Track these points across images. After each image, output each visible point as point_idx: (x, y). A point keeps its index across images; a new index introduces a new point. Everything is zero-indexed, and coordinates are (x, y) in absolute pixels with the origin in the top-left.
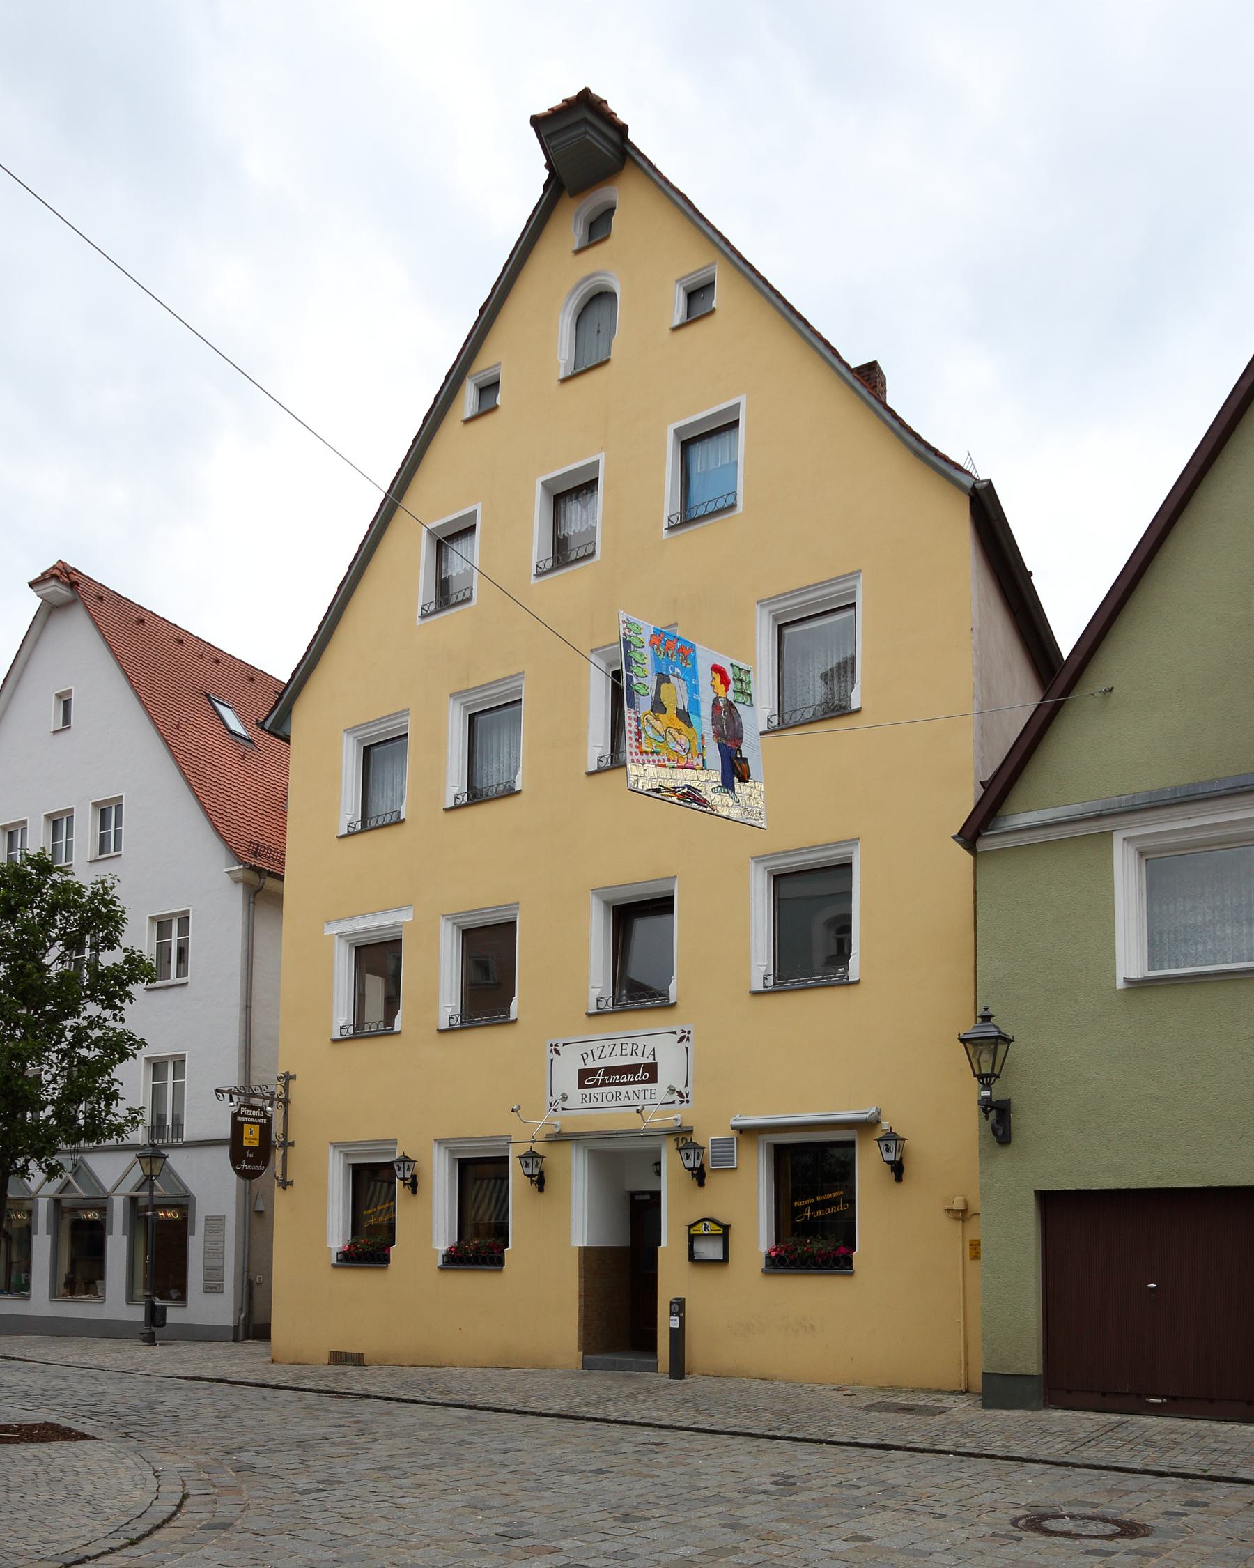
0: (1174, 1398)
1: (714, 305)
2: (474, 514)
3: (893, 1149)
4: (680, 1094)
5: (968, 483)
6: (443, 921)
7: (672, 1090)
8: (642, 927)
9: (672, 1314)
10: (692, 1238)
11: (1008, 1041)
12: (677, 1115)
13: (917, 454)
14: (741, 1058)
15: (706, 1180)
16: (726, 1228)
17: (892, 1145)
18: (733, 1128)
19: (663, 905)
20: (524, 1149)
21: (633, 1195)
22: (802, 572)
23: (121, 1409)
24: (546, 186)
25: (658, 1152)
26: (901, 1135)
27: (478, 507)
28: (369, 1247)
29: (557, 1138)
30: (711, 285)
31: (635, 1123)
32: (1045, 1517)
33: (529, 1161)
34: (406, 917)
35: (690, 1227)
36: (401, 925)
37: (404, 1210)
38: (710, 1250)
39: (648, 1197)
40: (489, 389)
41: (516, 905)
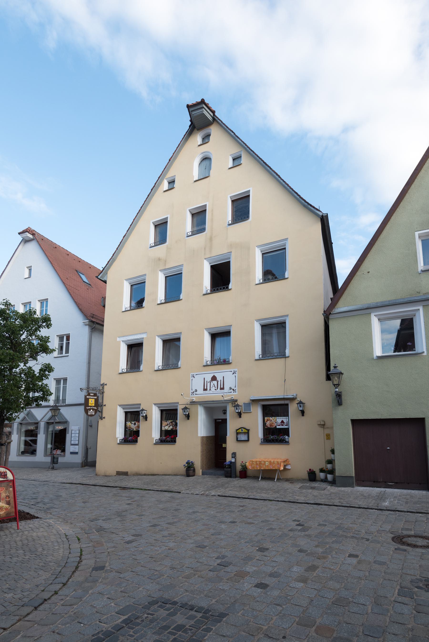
0: (397, 483)
1: (241, 162)
2: (167, 218)
3: (302, 406)
4: (233, 390)
5: (321, 214)
6: (157, 337)
7: (231, 388)
8: (218, 340)
9: (232, 458)
10: (237, 434)
11: (342, 374)
12: (233, 396)
13: (304, 206)
14: (249, 378)
15: (242, 416)
16: (248, 430)
17: (302, 405)
18: (251, 400)
19: (227, 334)
20: (183, 407)
21: (216, 420)
22: (271, 238)
23: (46, 500)
24: (190, 126)
25: (226, 407)
26: (303, 402)
27: (169, 216)
28: (131, 437)
29: (193, 403)
30: (240, 157)
31: (222, 399)
32: (404, 537)
33: (185, 410)
34: (144, 336)
35: (237, 430)
36: (143, 338)
37: (143, 426)
38: (243, 437)
39: (221, 421)
40: (172, 182)
41: (181, 333)
